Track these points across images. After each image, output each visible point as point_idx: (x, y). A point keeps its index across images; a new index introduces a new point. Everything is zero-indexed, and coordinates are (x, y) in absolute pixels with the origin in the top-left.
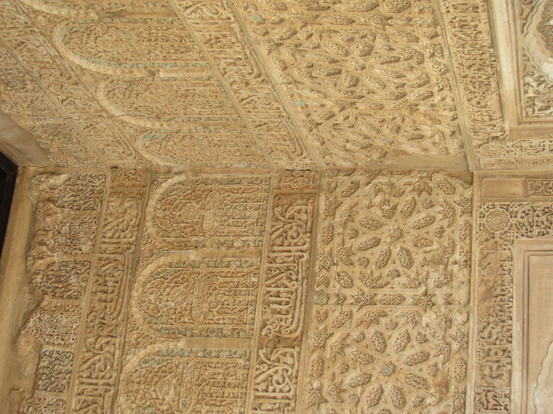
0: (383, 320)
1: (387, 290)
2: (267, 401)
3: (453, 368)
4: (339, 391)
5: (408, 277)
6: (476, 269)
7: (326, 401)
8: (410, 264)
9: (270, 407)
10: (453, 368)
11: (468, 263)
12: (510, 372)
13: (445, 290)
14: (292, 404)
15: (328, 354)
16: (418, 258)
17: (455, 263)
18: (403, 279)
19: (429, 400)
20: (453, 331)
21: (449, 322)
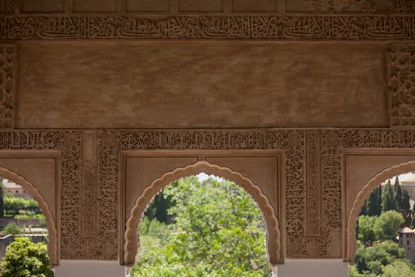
2: (410, 24)
7: (412, 55)
9: (407, 26)
14: (410, 37)
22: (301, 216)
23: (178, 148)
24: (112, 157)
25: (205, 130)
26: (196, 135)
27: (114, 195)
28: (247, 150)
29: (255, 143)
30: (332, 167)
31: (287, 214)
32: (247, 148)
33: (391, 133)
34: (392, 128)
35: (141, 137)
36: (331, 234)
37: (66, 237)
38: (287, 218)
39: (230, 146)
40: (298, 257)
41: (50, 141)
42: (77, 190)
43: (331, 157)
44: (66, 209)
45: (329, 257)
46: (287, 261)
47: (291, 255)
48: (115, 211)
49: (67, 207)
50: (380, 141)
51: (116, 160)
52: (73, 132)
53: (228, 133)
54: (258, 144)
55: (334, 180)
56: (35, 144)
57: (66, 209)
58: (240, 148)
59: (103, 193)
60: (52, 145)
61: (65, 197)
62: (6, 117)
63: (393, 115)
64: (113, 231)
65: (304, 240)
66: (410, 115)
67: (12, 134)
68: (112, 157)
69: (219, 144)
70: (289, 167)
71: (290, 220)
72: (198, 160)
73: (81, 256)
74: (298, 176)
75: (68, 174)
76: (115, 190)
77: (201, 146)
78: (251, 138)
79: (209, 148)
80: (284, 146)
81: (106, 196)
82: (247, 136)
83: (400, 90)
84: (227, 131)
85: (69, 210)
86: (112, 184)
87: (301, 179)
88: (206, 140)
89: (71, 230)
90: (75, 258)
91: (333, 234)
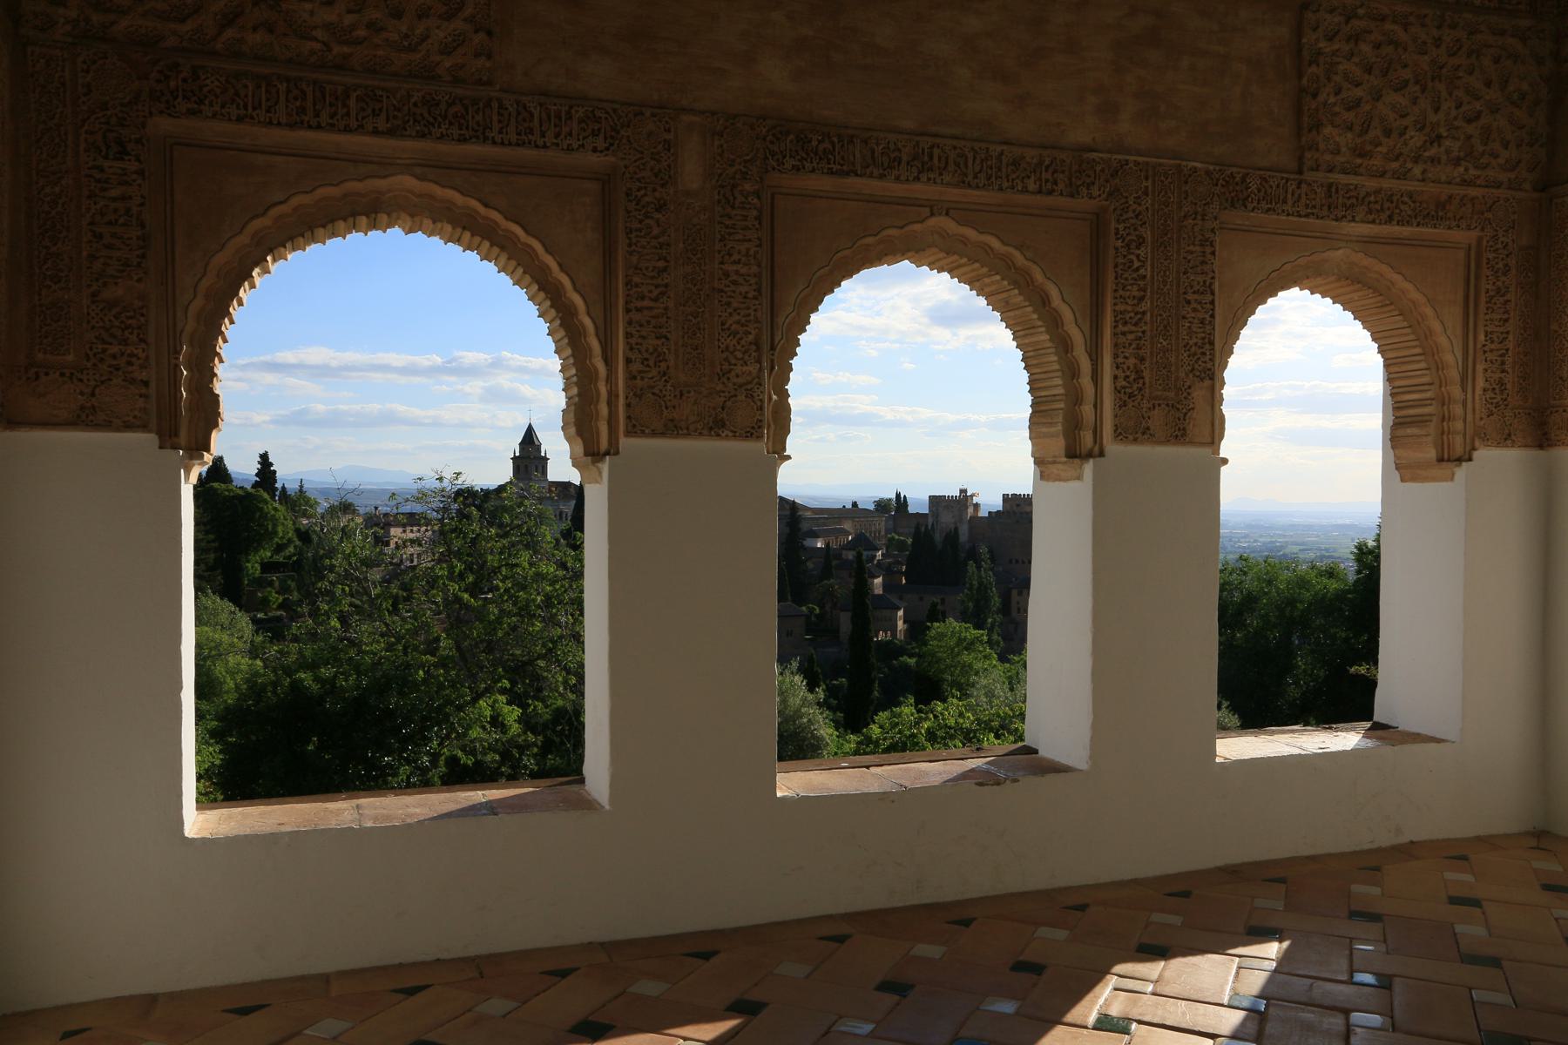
0: (1417, 88)
1: (1444, 94)
3: (1377, 162)
4: (1356, 38)
5: (1455, 118)
6: (1461, 191)
7: (1347, 22)
8: (1469, 121)
10: (1377, 162)
11: (1465, 183)
12: (1373, 222)
13: (1444, 158)
15: (1389, 26)
16: (1470, 129)
17: (1466, 170)
18: (1454, 113)
19: (1349, 135)
20: (1409, 165)
21: (1416, 160)
22: (1141, 352)
23: (897, 179)
24: (748, 187)
25: (955, 142)
26: (936, 151)
27: (753, 281)
28: (1038, 197)
29: (1055, 183)
30: (1198, 248)
31: (1116, 345)
32: (1040, 192)
33: (1304, 186)
34: (1309, 176)
35: (814, 143)
36: (1195, 394)
37: (638, 382)
38: (1116, 356)
39: (1006, 185)
40: (1135, 440)
41: (595, 134)
42: (661, 264)
43: (1196, 229)
44: (638, 310)
45: (1192, 443)
46: (1113, 448)
47: (1121, 434)
48: (757, 321)
49: (639, 304)
50: (1285, 202)
51: (758, 194)
52: (653, 115)
53: (1002, 153)
54: (1061, 186)
55: (1200, 279)
56: (557, 136)
57: (638, 310)
58: (1025, 190)
59: (727, 275)
60: (600, 143)
61: (636, 279)
62: (477, 55)
63: (1310, 149)
64: (753, 368)
65: (1145, 404)
66: (1338, 152)
67: (495, 105)
68: (748, 187)
69: (982, 176)
70: (1119, 243)
71: (1120, 360)
72: (932, 214)
73: (673, 429)
74: (1137, 264)
75: (641, 222)
76: (755, 269)
77: (947, 178)
78: (1047, 168)
79: (963, 184)
80: (1110, 194)
81: (735, 283)
82: (1041, 163)
83: (1321, 98)
84: (999, 148)
85: (646, 312)
86: (747, 255)
87: (1142, 271)
88: (957, 164)
89: (651, 363)
90: (663, 434)
91: (1198, 394)
